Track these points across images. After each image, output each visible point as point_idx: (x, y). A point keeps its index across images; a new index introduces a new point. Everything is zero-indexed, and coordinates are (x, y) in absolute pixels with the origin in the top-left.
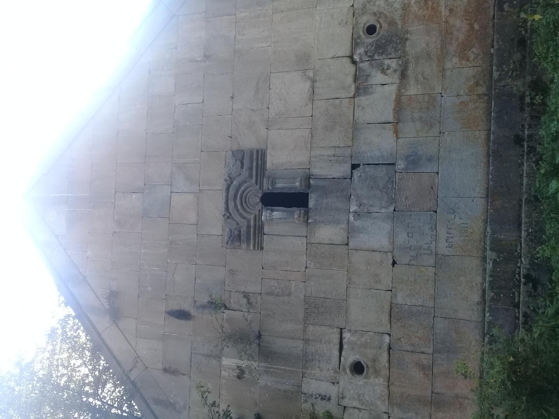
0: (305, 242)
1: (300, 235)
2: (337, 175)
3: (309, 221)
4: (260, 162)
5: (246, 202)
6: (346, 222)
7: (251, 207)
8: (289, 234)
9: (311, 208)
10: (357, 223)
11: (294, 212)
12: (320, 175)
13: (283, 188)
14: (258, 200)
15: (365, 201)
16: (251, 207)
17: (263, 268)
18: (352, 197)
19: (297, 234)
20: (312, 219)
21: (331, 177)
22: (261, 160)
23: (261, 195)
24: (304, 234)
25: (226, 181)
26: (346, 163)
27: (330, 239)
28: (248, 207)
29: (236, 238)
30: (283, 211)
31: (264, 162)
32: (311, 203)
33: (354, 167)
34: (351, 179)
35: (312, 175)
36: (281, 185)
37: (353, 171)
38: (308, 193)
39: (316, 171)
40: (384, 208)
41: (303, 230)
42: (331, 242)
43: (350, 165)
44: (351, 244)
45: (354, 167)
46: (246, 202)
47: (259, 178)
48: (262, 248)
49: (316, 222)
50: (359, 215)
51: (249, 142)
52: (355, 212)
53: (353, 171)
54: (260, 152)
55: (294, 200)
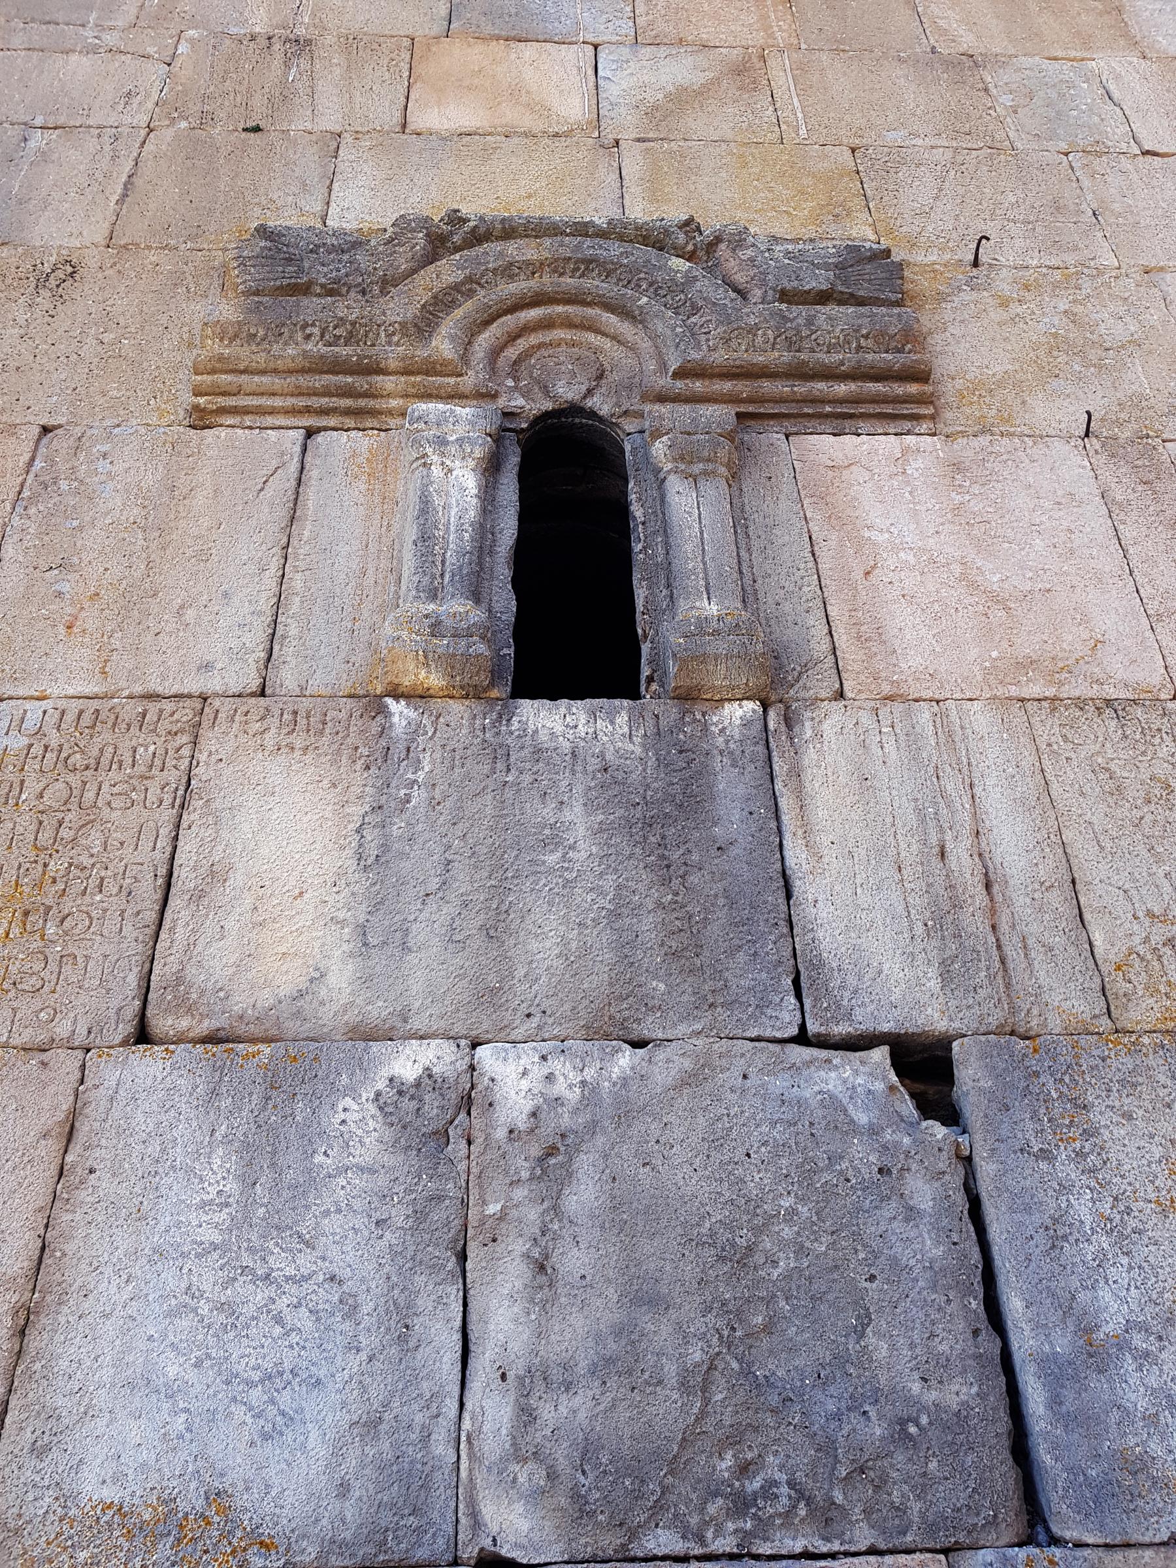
0: (214, 684)
1: (286, 652)
2: (824, 912)
3: (396, 707)
4: (842, 389)
5: (547, 324)
6: (378, 1011)
7: (512, 353)
8: (297, 581)
9: (506, 716)
10: (356, 1122)
11: (476, 597)
12: (796, 773)
13: (665, 528)
14: (567, 391)
15: (584, 1195)
16: (512, 353)
17: (46, 430)
18: (626, 1058)
19: (290, 627)
20: (415, 730)
21: (796, 855)
22: (856, 400)
23: (605, 410)
24: (287, 677)
25: (689, 225)
26: (946, 976)
27: (216, 875)
28: (513, 338)
29: (288, 272)
30: (484, 531)
31: (843, 418)
32: (550, 720)
33: (924, 1068)
34: (802, 1038)
35: (789, 721)
36: (684, 517)
37: (880, 1055)
38: (635, 695)
39: (830, 745)
40: (526, 1416)
41: (318, 664)
42: (184, 877)
43: (932, 1016)
44: (147, 1065)
45: (924, 1068)
46: (547, 324)
47: (727, 386)
48: (201, 419)
49: (386, 757)
50: (442, 1136)
51: (968, 344)
52: (469, 1098)
53: (880, 1055)
54: (913, 388)
55: (570, 595)
